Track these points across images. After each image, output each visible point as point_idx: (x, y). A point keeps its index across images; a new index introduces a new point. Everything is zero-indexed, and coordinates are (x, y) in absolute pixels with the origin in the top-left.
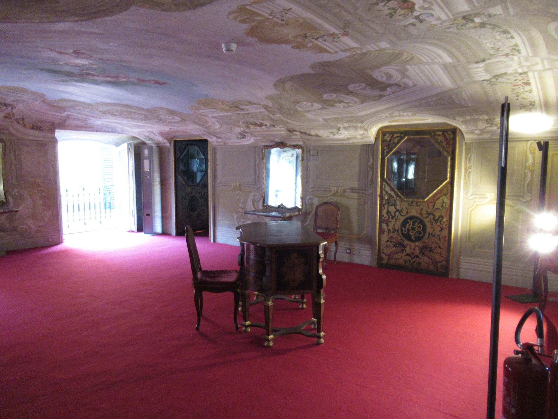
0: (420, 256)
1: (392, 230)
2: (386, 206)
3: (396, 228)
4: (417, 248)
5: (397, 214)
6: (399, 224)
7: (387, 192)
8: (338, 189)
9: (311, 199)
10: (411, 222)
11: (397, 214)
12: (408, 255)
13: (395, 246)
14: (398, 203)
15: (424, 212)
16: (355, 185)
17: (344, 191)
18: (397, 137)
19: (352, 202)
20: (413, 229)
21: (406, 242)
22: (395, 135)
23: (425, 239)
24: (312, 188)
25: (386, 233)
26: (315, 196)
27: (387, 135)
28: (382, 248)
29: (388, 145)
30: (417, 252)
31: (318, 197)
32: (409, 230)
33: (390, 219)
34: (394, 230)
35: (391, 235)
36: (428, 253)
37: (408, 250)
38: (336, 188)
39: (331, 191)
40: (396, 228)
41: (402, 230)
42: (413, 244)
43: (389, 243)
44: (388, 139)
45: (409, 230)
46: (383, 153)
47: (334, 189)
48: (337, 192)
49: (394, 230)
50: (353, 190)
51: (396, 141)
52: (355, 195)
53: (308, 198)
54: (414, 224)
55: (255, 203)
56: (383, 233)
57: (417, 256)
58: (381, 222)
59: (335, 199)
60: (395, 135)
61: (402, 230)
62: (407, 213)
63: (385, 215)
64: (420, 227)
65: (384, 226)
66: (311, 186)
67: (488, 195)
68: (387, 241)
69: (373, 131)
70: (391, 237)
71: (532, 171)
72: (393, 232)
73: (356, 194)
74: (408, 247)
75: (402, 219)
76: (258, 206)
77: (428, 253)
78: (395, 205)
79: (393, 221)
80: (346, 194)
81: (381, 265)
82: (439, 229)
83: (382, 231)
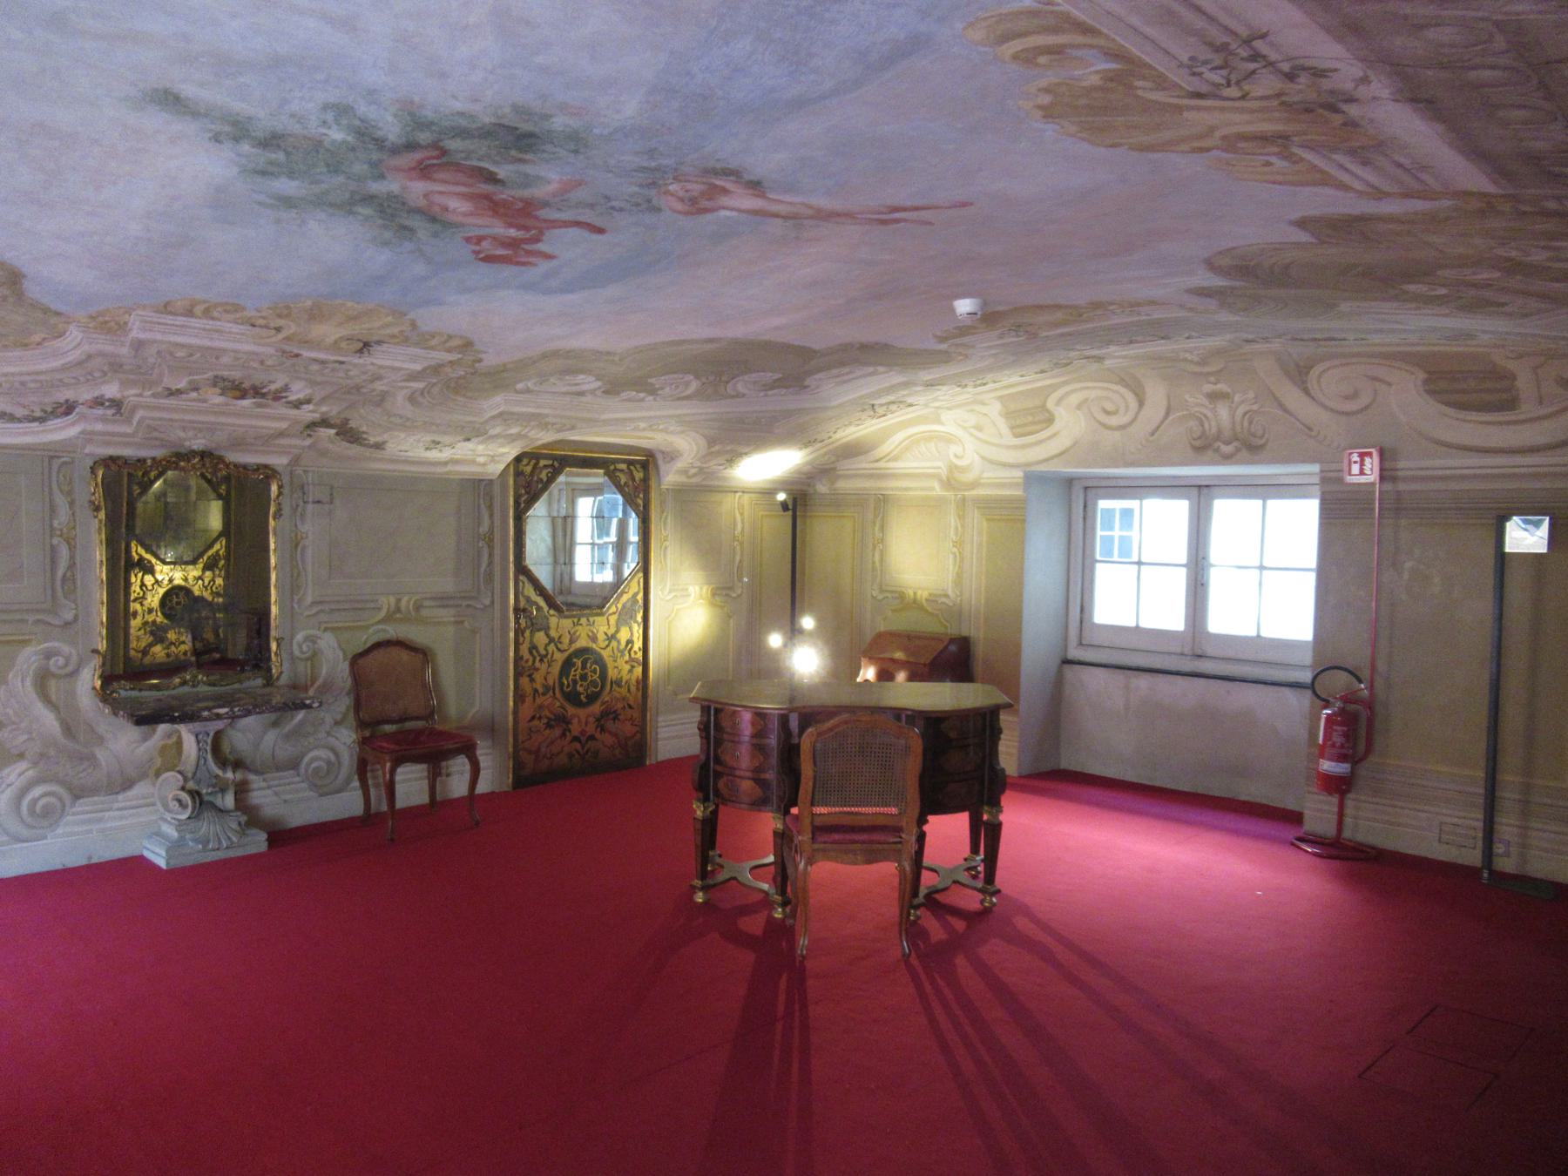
0: (598, 735)
1: (541, 690)
2: (527, 633)
3: (551, 682)
4: (591, 719)
5: (552, 647)
6: (556, 669)
7: (528, 599)
8: (399, 600)
9: (312, 639)
10: (579, 663)
11: (552, 647)
12: (576, 739)
13: (548, 726)
14: (553, 621)
15: (601, 637)
16: (448, 585)
17: (418, 607)
18: (546, 466)
19: (438, 634)
20: (584, 678)
21: (571, 710)
22: (542, 463)
23: (605, 697)
24: (314, 603)
25: (529, 700)
26: (326, 630)
27: (525, 461)
28: (521, 738)
29: (528, 486)
30: (591, 729)
31: (333, 629)
32: (575, 682)
33: (537, 664)
34: (547, 688)
35: (539, 701)
36: (610, 725)
37: (575, 728)
38: (392, 600)
39: (380, 609)
40: (551, 682)
41: (562, 685)
42: (582, 713)
43: (536, 722)
44: (528, 469)
45: (575, 682)
46: (517, 503)
47: (387, 602)
48: (398, 610)
49: (547, 688)
50: (443, 600)
51: (543, 476)
52: (447, 615)
53: (299, 637)
54: (584, 667)
55: (53, 685)
56: (523, 701)
57: (592, 738)
58: (518, 675)
59: (391, 631)
60: (542, 463)
61: (562, 685)
62: (572, 642)
63: (526, 655)
64: (594, 671)
65: (525, 681)
66: (309, 600)
67: (691, 589)
68: (533, 718)
69: (510, 452)
70: (541, 707)
71: (741, 544)
72: (544, 694)
73: (452, 611)
74: (575, 721)
75: (560, 658)
76: (72, 693)
77: (610, 725)
78: (547, 629)
79: (544, 667)
80: (425, 612)
81: (520, 782)
82: (628, 667)
83: (520, 697)
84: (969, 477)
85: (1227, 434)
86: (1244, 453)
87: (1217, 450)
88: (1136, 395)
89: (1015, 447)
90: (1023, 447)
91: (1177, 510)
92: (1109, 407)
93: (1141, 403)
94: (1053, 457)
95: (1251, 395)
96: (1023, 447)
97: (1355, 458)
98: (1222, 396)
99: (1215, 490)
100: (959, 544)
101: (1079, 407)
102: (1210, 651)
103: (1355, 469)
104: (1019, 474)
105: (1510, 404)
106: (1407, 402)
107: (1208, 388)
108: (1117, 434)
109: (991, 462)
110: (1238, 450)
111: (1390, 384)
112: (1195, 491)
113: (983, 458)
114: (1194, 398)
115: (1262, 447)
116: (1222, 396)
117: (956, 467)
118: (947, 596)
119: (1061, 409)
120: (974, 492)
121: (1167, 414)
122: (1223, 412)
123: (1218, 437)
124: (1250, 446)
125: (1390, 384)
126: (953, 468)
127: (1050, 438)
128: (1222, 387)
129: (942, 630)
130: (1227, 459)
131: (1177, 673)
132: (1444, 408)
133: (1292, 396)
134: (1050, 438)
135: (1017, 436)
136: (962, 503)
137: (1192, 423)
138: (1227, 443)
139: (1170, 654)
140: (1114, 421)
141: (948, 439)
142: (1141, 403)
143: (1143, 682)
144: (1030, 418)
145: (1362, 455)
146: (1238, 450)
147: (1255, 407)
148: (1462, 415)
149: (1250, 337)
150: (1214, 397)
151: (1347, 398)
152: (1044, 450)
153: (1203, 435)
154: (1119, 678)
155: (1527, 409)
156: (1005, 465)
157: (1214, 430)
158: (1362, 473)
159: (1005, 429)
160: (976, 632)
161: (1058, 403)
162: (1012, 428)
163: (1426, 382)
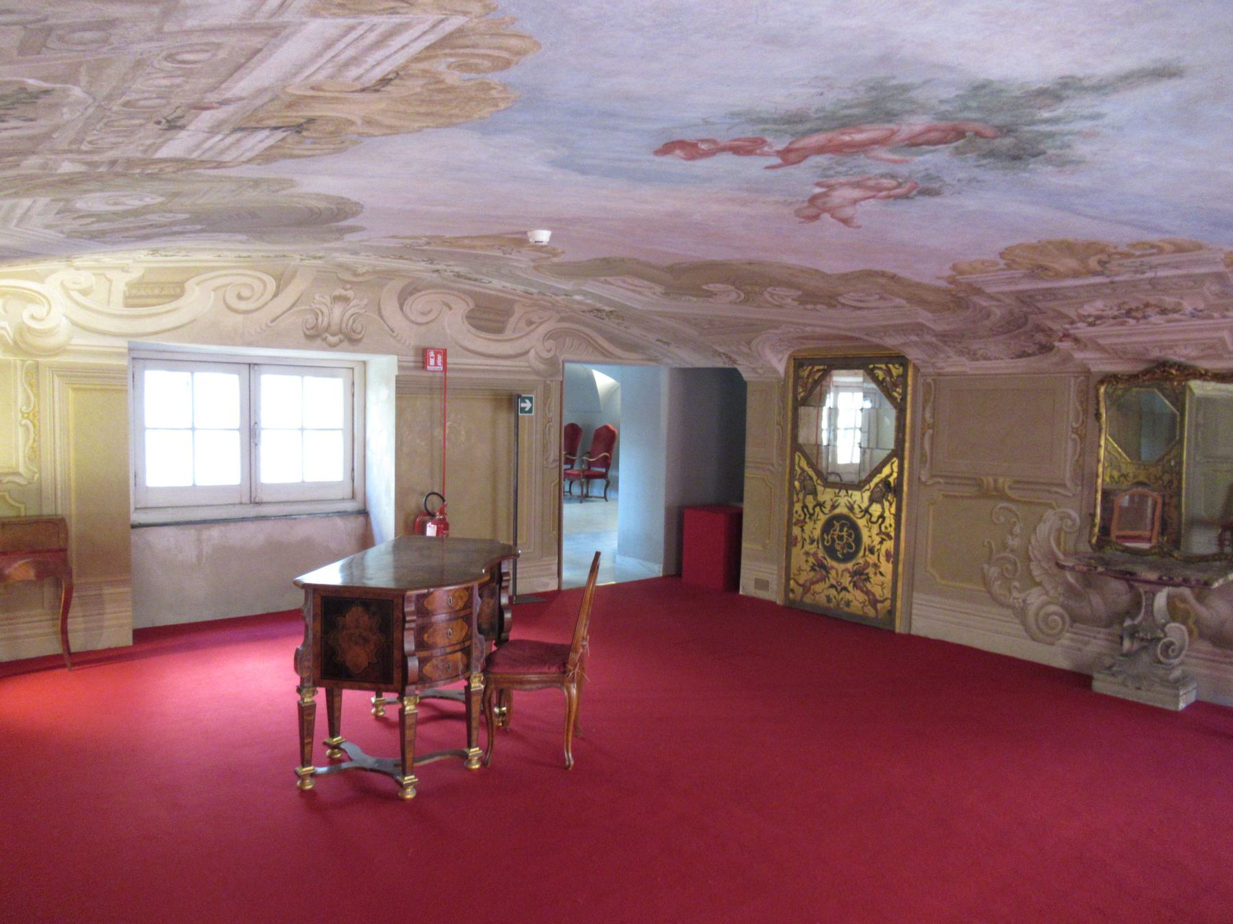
84: (51, 342)
85: (334, 328)
86: (346, 344)
87: (325, 339)
88: (278, 287)
89: (121, 316)
90: (128, 317)
91: (228, 384)
92: (245, 293)
93: (275, 295)
94: (169, 330)
95: (365, 301)
96: (128, 317)
97: (432, 354)
98: (346, 299)
99: (263, 368)
100: (34, 417)
101: (215, 290)
102: (265, 500)
103: (432, 362)
104: (122, 344)
105: (500, 331)
106: (452, 325)
107: (339, 292)
108: (240, 318)
109: (84, 328)
110: (341, 341)
111: (450, 308)
112: (245, 369)
113: (74, 324)
114: (321, 300)
115: (359, 341)
116: (346, 299)
117: (29, 329)
118: (20, 475)
119: (197, 289)
120: (56, 359)
121: (294, 305)
122: (337, 310)
123: (327, 329)
124: (351, 339)
125: (450, 308)
126: (22, 330)
127: (168, 312)
128: (350, 294)
129: (13, 513)
130: (333, 347)
131: (244, 519)
132: (473, 330)
133: (390, 308)
134: (168, 312)
135: (127, 306)
136: (34, 375)
137: (310, 318)
138: (333, 335)
139: (234, 504)
140: (243, 306)
141: (27, 298)
142: (275, 295)
143: (215, 532)
144: (157, 292)
145: (436, 354)
146: (341, 341)
147: (362, 311)
148: (484, 335)
149: (462, 270)
150: (337, 299)
151: (423, 314)
152: (153, 322)
153: (315, 327)
154: (192, 532)
155: (508, 333)
156: (103, 333)
157: (325, 323)
158: (436, 364)
159: (118, 298)
160: (68, 508)
161: (198, 284)
162: (126, 298)
163: (472, 310)
